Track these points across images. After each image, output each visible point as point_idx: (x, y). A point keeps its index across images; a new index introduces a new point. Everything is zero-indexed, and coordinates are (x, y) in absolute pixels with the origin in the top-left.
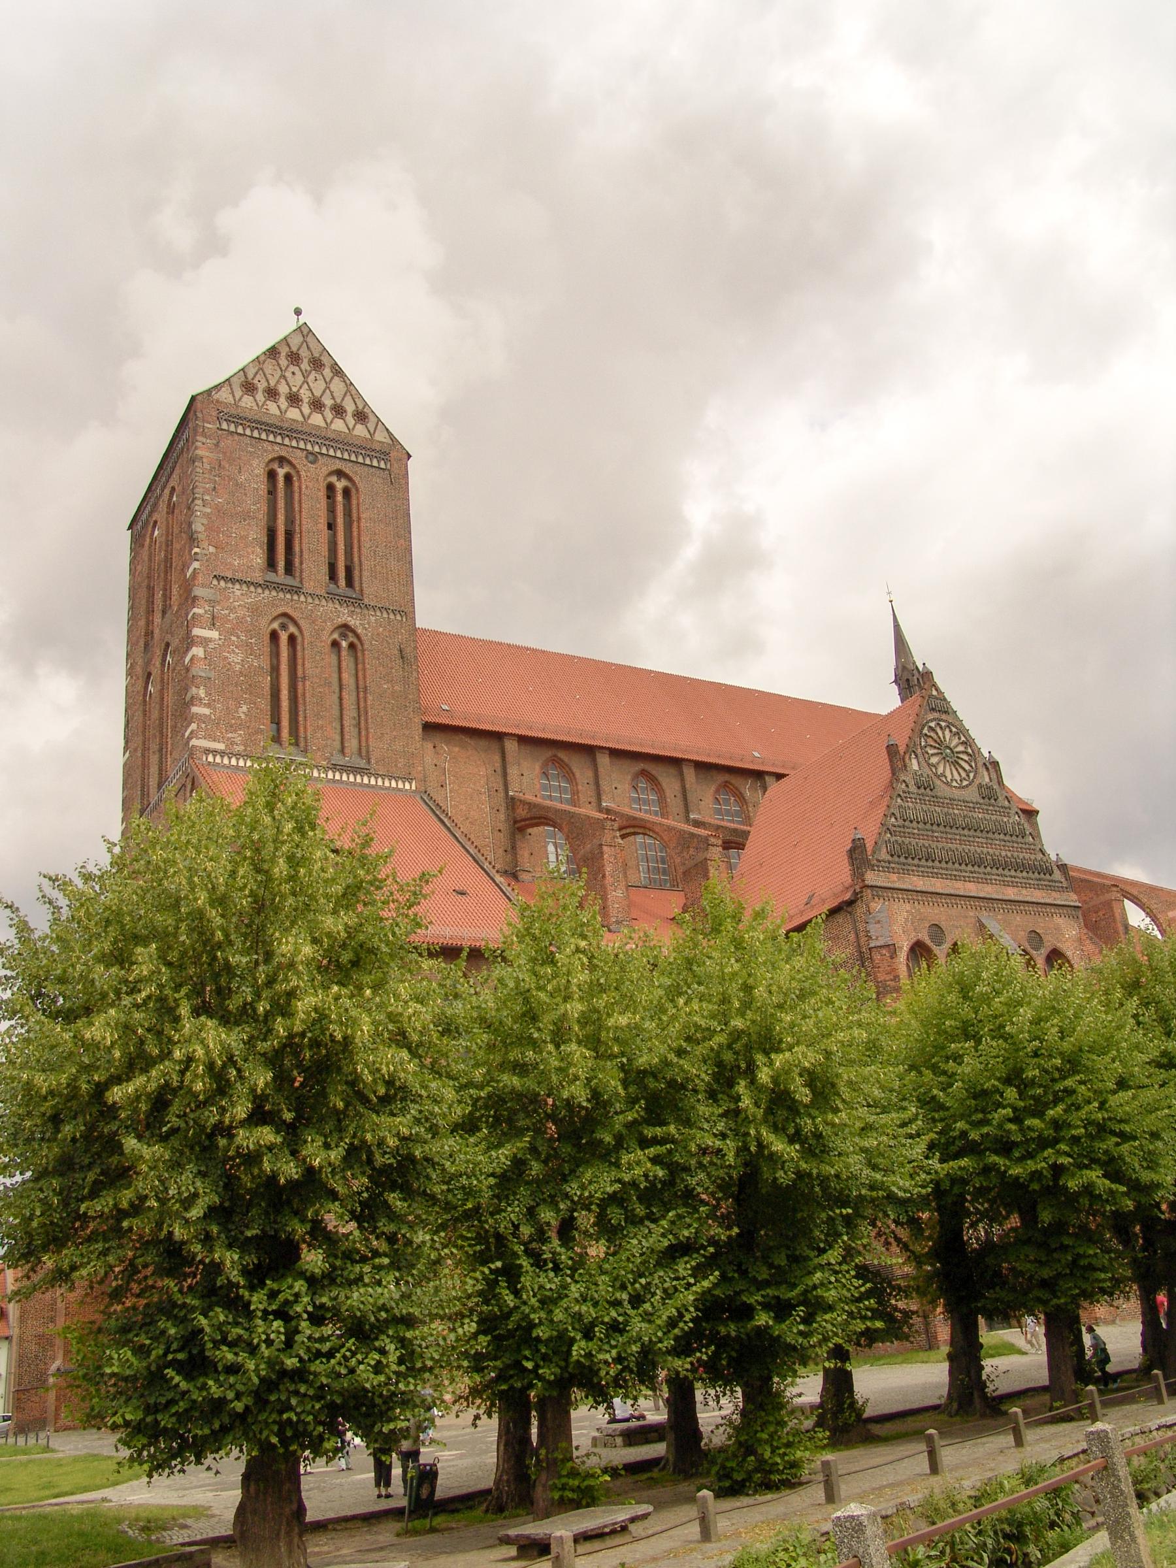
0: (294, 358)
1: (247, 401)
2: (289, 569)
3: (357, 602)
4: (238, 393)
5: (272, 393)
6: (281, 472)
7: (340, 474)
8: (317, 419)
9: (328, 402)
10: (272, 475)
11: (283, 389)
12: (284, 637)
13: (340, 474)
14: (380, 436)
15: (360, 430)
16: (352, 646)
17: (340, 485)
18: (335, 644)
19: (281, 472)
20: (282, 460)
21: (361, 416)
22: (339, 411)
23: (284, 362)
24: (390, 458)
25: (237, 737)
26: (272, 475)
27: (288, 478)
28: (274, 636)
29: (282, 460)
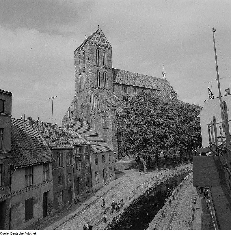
0: (99, 33)
1: (94, 41)
2: (99, 64)
3: (105, 68)
4: (93, 39)
5: (97, 39)
6: (98, 50)
7: (104, 50)
8: (102, 43)
9: (103, 40)
10: (97, 50)
11: (98, 39)
12: (99, 72)
13: (104, 50)
14: (109, 45)
15: (107, 44)
16: (106, 73)
17: (104, 52)
18: (104, 73)
19: (98, 50)
20: (98, 49)
21: (107, 42)
22: (104, 41)
23: (98, 34)
24: (109, 48)
25: (94, 85)
26: (97, 50)
27: (99, 51)
28: (97, 72)
29: (98, 49)
